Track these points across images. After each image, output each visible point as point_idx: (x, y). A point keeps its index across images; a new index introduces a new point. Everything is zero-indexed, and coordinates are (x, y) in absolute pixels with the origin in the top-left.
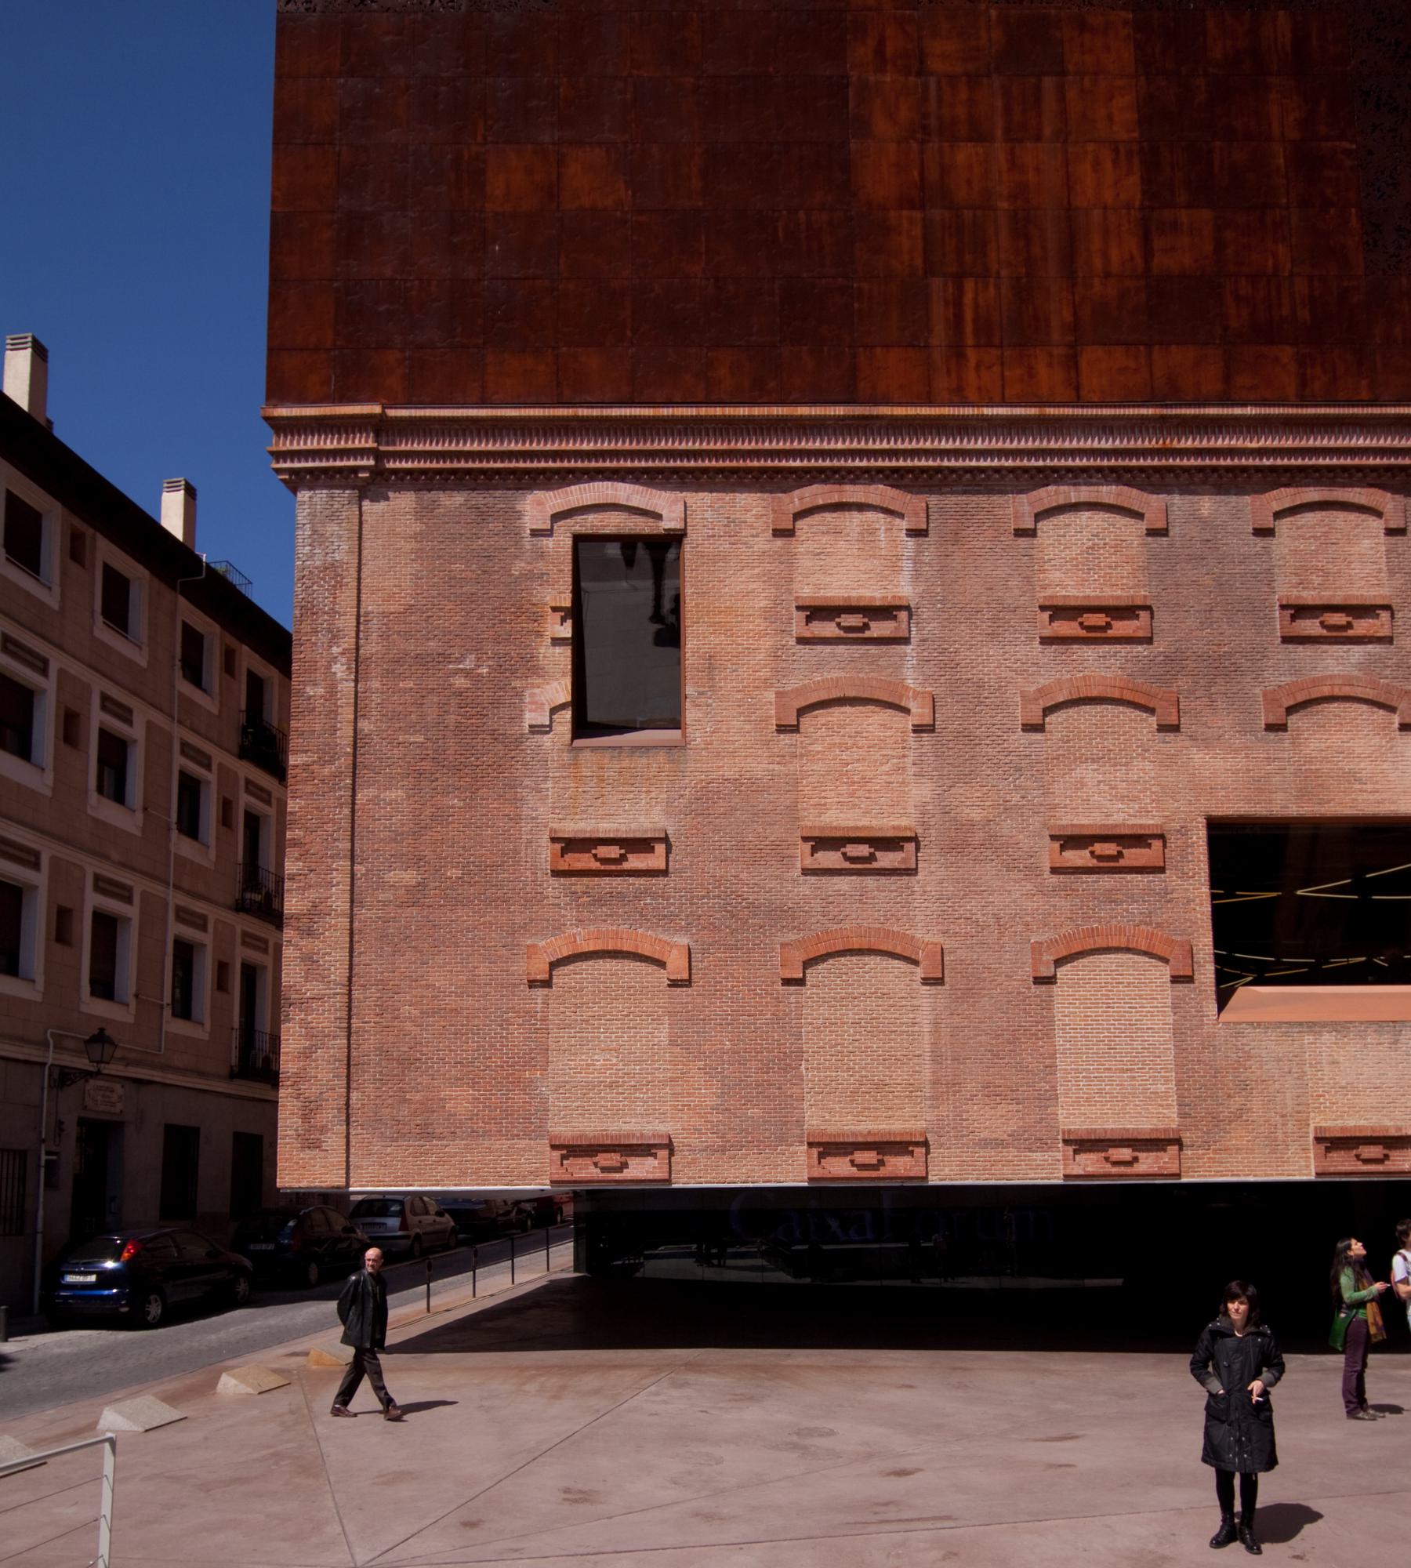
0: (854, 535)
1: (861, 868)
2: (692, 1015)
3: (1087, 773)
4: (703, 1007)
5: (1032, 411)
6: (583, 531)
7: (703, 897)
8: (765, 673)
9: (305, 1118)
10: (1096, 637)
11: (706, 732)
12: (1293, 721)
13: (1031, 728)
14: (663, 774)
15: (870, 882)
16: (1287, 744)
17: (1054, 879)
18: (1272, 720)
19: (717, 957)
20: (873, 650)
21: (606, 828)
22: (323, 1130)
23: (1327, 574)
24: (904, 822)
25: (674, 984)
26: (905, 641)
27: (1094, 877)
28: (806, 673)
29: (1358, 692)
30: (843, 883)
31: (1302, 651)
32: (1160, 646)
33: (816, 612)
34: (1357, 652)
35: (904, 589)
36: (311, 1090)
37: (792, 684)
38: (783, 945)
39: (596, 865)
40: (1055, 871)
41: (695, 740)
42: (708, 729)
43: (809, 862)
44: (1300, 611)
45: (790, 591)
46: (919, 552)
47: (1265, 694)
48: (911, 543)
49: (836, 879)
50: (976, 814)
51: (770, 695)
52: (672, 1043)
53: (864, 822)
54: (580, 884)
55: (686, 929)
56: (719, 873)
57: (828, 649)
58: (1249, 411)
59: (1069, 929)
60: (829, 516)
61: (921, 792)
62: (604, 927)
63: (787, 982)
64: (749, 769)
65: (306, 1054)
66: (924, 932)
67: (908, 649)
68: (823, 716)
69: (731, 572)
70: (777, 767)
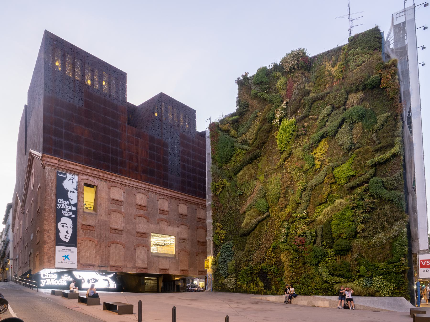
1: (116, 233)
3: (140, 225)
6: (85, 182)
9: (48, 259)
10: (141, 209)
12: (160, 223)
13: (135, 219)
15: (118, 235)
17: (136, 237)
20: (119, 206)
21: (88, 224)
22: (51, 260)
24: (122, 228)
25: (96, 245)
26: (122, 206)
30: (115, 235)
31: (160, 215)
32: (147, 212)
33: (113, 200)
34: (165, 216)
35: (122, 199)
36: (49, 255)
38: (108, 242)
39: (86, 228)
40: (136, 236)
43: (111, 232)
45: (110, 196)
46: (124, 195)
48: (123, 194)
49: (114, 234)
50: (129, 229)
52: (95, 253)
53: (117, 228)
54: (85, 231)
55: (97, 238)
61: (123, 225)
62: (88, 237)
63: (109, 246)
65: (48, 250)
66: (123, 242)
67: (123, 207)
68: (115, 213)
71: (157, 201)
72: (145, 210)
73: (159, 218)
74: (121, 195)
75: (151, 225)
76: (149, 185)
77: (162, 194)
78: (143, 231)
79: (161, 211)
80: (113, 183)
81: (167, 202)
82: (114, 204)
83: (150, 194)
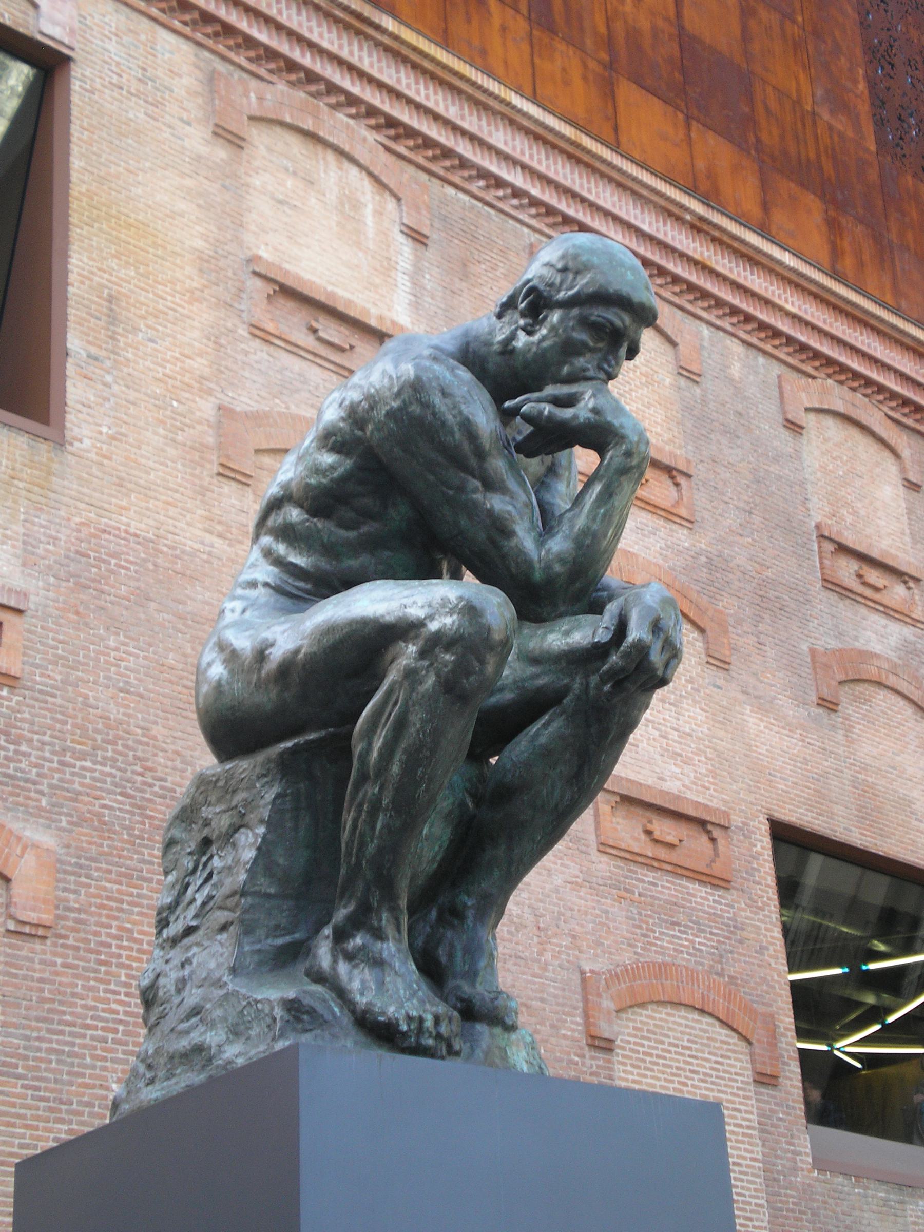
0: (332, 197)
2: (51, 1011)
4: (74, 995)
5: (568, 131)
7: (82, 756)
8: (200, 365)
11: (101, 433)
14: (21, 485)
16: (840, 737)
17: (604, 865)
18: (826, 693)
19: (105, 889)
23: (855, 513)
27: (650, 876)
28: (263, 394)
29: (903, 687)
31: (844, 608)
37: (244, 402)
41: (81, 441)
42: (104, 430)
44: (843, 549)
47: (813, 652)
48: (405, 249)
51: (206, 408)
55: (47, 816)
56: (115, 713)
57: (296, 364)
58: (787, 259)
59: (626, 958)
60: (295, 144)
64: (171, 529)
69: (148, 164)
70: (218, 542)
71: (785, 435)
72: (668, 514)
73: (833, 644)
74: (387, 268)
75: (752, 721)
76: (699, 227)
77: (830, 362)
78: (673, 786)
79: (846, 570)
80: (281, 87)
81: (891, 466)
82: (293, 348)
83: (706, 331)
